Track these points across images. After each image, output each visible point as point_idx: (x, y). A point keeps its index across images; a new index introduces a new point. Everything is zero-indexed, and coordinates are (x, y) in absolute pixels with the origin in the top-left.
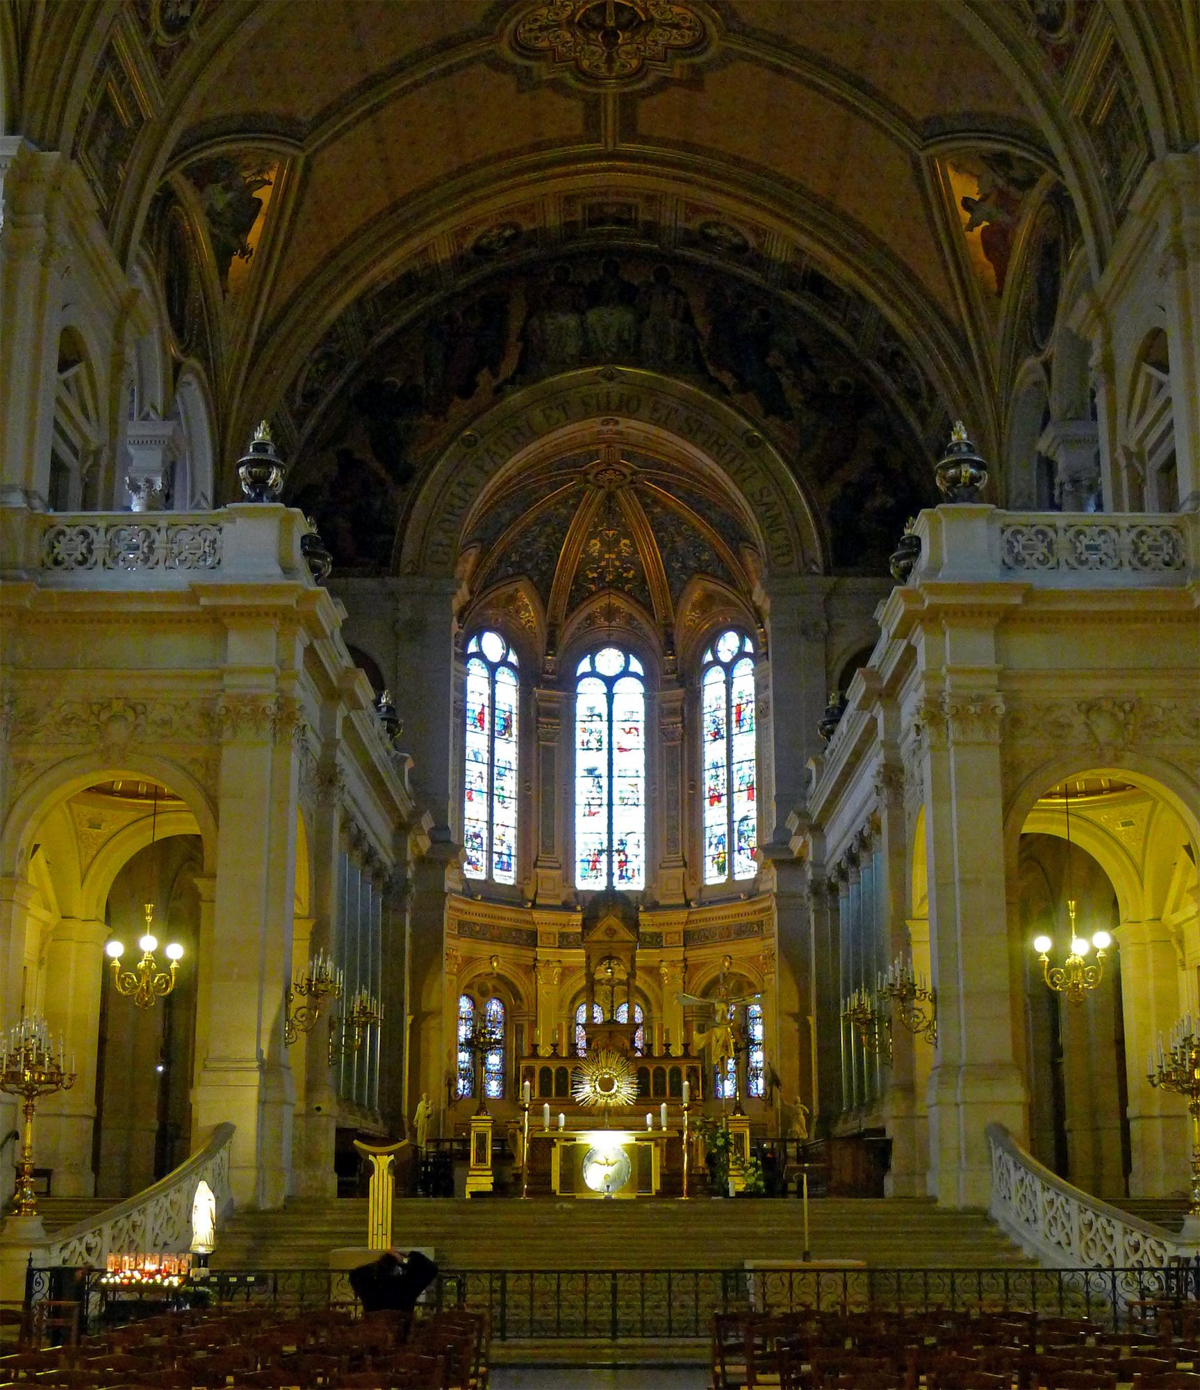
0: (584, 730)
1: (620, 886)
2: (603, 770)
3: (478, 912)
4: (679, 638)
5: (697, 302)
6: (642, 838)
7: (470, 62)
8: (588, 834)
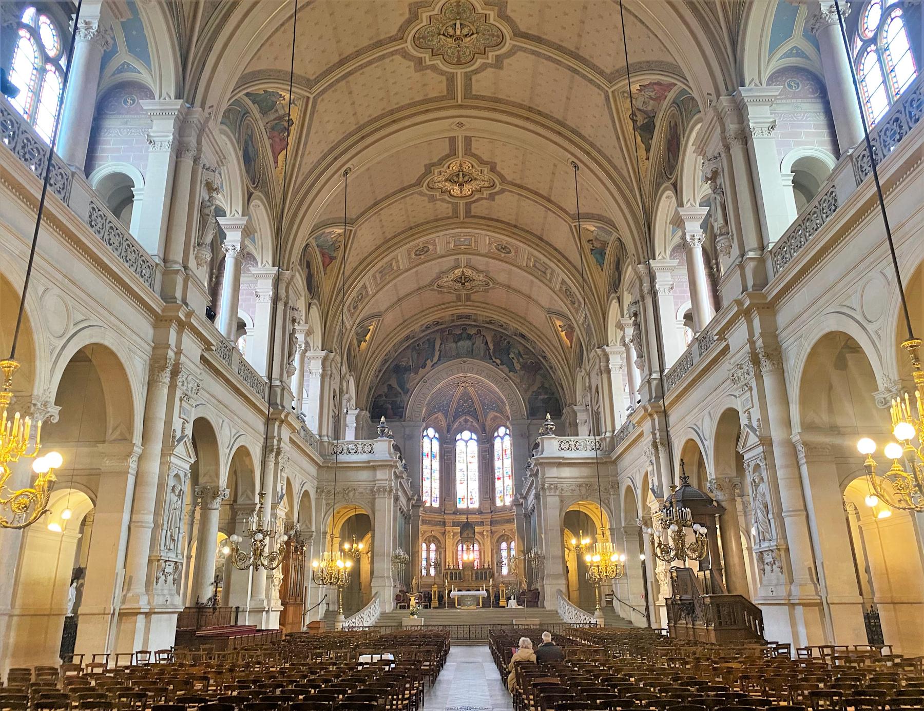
1: (471, 506)
3: (427, 517)
4: (487, 428)
5: (489, 340)
8: (461, 491)
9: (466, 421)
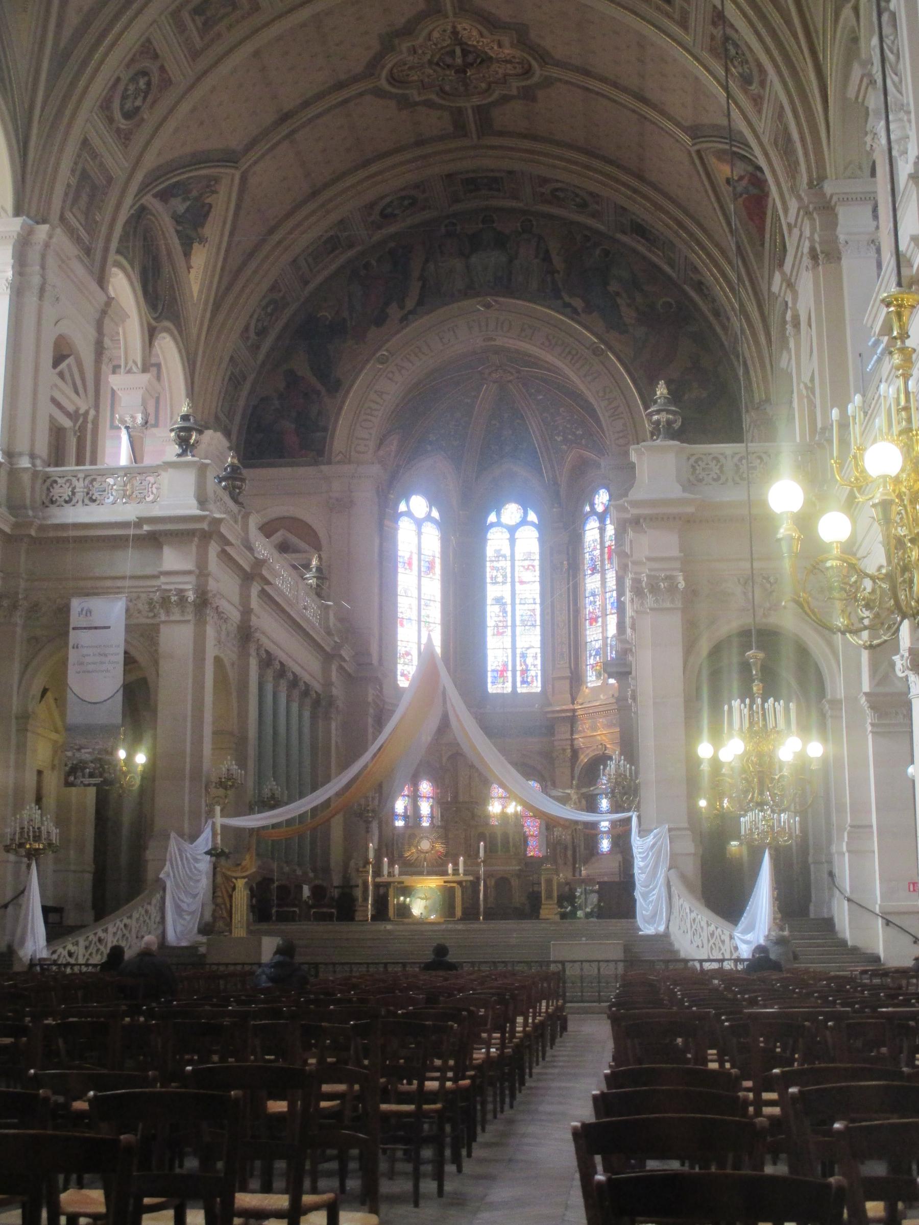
0: (493, 568)
2: (508, 599)
6: (539, 651)
7: (361, 95)
8: (496, 652)
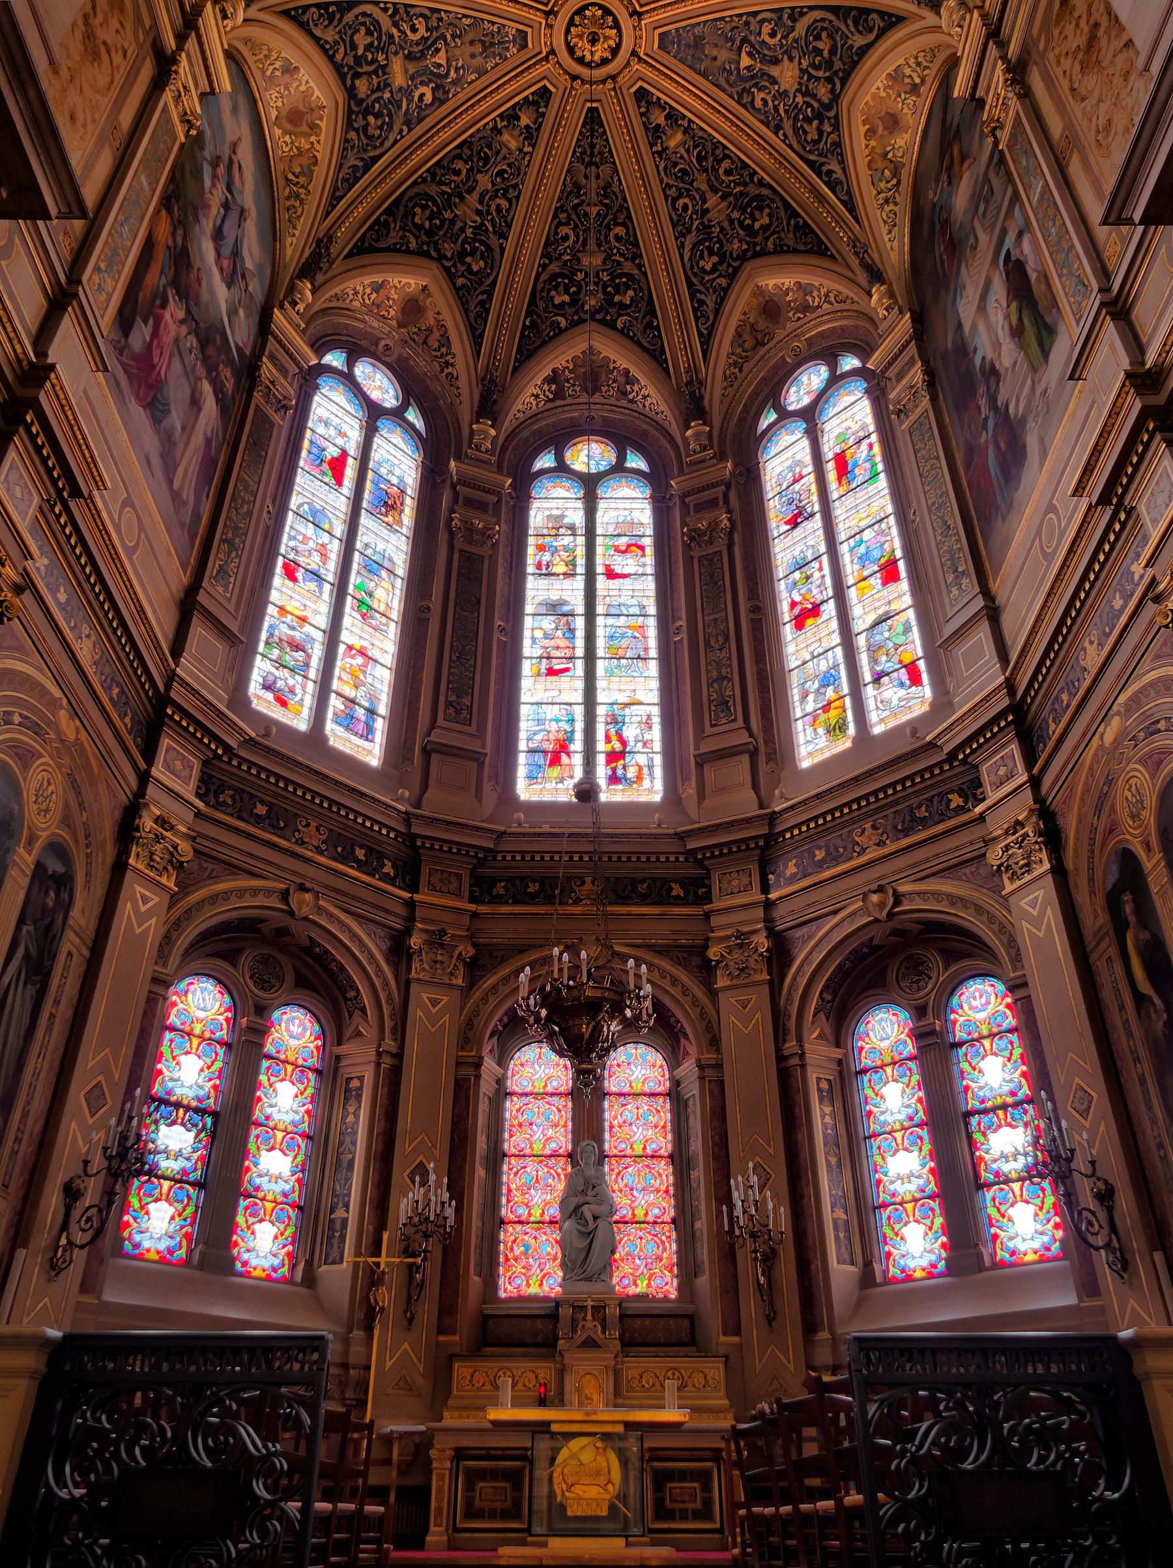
4: (714, 395)
9: (592, 374)
